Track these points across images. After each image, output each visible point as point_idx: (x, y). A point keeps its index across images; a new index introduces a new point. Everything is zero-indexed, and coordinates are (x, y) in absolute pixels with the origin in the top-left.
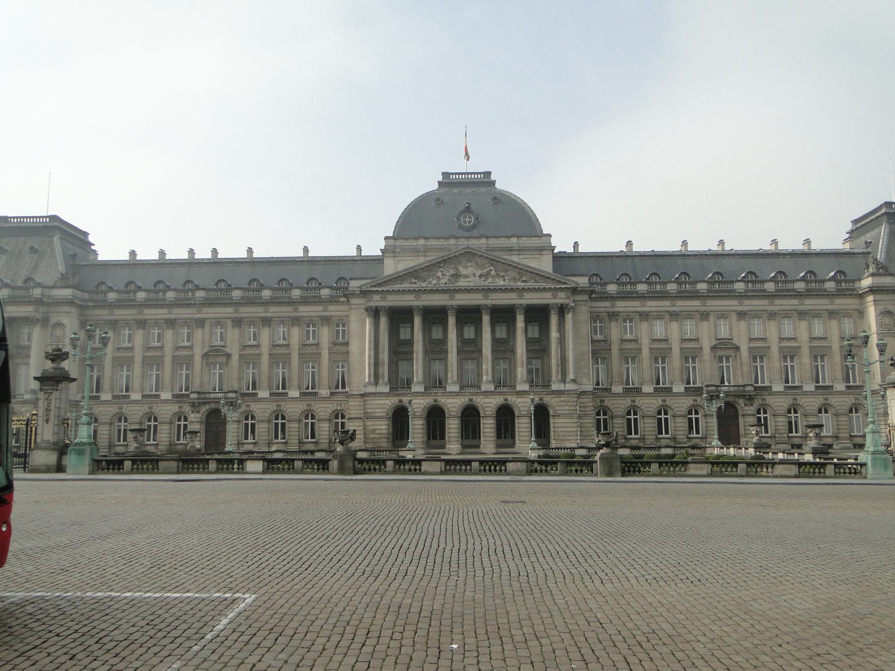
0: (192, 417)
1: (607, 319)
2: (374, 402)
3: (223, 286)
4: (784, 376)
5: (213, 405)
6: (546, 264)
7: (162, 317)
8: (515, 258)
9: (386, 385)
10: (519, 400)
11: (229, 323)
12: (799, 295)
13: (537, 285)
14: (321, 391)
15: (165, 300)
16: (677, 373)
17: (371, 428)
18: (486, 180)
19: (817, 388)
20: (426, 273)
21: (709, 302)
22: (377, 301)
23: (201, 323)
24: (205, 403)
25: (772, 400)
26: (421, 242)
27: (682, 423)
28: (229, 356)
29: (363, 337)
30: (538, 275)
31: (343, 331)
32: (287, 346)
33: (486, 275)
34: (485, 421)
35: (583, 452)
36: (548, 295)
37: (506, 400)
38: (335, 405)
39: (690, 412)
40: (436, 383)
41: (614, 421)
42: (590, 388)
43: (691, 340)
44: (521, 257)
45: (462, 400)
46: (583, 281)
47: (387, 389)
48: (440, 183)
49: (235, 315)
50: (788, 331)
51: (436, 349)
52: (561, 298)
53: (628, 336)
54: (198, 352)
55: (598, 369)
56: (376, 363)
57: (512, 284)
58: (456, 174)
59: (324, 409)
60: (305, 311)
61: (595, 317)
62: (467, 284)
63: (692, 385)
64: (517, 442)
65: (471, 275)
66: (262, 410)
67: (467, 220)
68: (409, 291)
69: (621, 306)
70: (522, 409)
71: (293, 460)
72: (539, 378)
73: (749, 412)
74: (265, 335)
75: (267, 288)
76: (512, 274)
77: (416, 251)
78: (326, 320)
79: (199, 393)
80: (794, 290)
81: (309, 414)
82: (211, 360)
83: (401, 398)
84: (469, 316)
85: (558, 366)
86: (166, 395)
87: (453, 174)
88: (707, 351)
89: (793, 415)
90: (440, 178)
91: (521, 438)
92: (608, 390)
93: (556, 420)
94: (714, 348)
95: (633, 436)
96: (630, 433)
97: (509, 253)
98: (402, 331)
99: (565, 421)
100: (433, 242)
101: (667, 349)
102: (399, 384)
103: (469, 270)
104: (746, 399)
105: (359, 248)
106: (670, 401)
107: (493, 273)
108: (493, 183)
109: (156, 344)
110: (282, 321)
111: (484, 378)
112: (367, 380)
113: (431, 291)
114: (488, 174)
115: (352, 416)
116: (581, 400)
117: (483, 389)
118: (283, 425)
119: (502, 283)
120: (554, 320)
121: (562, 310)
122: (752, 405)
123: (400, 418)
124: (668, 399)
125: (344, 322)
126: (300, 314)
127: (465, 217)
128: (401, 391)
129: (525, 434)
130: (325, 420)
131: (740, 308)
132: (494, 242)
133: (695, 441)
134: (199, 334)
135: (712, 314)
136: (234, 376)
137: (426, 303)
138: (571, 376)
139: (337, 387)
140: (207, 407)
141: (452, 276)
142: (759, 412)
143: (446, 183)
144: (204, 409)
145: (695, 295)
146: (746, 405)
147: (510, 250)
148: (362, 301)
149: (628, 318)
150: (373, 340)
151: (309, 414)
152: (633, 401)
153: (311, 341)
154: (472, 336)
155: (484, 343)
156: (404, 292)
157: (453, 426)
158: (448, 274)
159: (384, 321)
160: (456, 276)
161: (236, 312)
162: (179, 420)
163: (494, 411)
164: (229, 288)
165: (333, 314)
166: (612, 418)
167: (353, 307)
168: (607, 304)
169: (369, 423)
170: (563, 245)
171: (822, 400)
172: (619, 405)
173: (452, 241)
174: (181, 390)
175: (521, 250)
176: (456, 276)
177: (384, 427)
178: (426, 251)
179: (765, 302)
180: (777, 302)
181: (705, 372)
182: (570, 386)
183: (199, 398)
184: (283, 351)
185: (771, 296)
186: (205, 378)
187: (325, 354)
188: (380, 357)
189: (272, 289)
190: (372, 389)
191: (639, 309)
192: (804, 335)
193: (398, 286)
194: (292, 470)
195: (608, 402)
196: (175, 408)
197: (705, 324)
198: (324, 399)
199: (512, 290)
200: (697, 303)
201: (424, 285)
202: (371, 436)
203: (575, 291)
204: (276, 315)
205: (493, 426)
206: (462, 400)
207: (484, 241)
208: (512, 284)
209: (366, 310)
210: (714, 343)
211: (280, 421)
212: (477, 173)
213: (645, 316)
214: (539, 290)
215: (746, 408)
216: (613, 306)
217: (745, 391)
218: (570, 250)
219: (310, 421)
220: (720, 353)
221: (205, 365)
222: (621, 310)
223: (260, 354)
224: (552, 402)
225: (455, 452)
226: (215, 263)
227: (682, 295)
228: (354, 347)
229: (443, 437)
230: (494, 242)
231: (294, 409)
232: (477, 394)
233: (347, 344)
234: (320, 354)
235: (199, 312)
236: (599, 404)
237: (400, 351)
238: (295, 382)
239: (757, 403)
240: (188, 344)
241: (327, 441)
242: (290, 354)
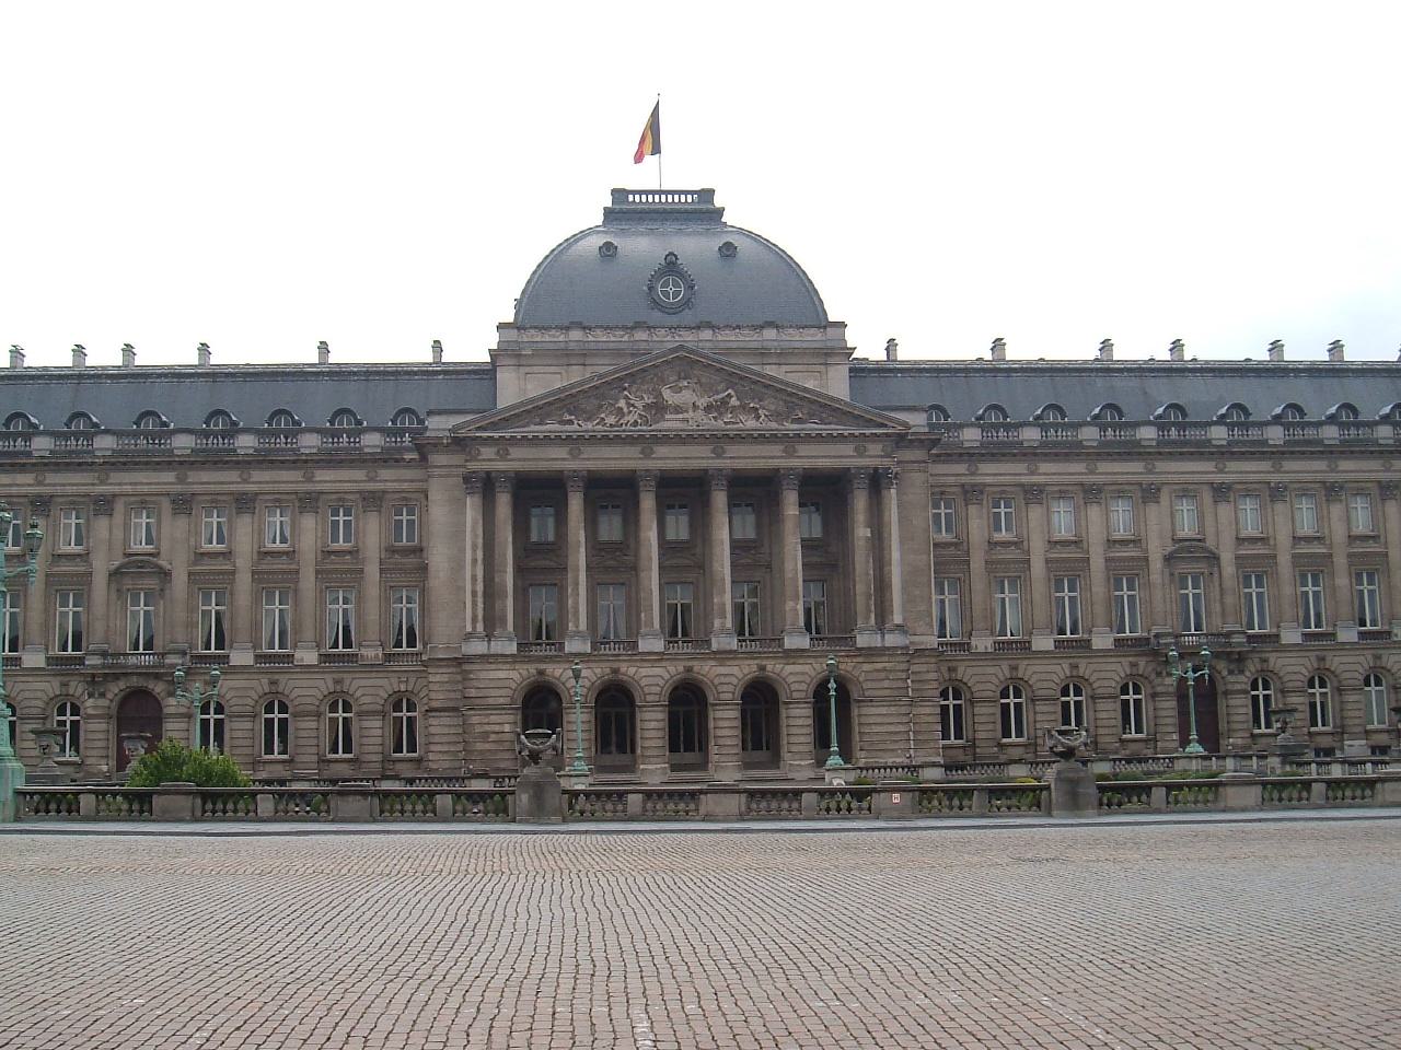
0: (89, 705)
1: (960, 501)
2: (483, 675)
3: (150, 425)
4: (1301, 614)
5: (135, 682)
6: (837, 385)
7: (24, 490)
8: (771, 371)
9: (511, 640)
10: (789, 668)
11: (166, 504)
12: (1329, 452)
13: (824, 429)
14: (364, 651)
15: (29, 454)
16: (1100, 609)
17: (478, 729)
18: (703, 207)
19: (1362, 635)
20: (596, 402)
21: (1161, 466)
22: (488, 460)
23: (104, 505)
24: (116, 677)
26: (576, 335)
27: (1109, 712)
28: (165, 575)
29: (457, 536)
30: (824, 407)
31: (411, 523)
32: (290, 554)
34: (719, 714)
35: (937, 773)
36: (848, 449)
37: (762, 668)
38: (394, 681)
39: (1125, 690)
40: (614, 639)
41: (977, 710)
42: (932, 641)
43: (1123, 542)
44: (784, 368)
45: (672, 669)
46: (917, 421)
47: (512, 648)
48: (608, 212)
49: (179, 488)
50: (1306, 524)
51: (614, 563)
52: (874, 456)
53: (1003, 535)
54: (101, 566)
55: (942, 602)
56: (491, 592)
57: (774, 425)
58: (640, 193)
59: (369, 690)
60: (326, 479)
61: (939, 495)
62: (679, 425)
63: (1128, 634)
64: (785, 755)
65: (688, 406)
66: (239, 691)
67: (671, 289)
68: (559, 440)
69: (991, 473)
70: (795, 687)
71: (432, 794)
72: (830, 625)
73: (1238, 687)
74: (244, 529)
75: (246, 431)
76: (771, 404)
77: (565, 356)
78: (372, 500)
79: (104, 654)
80: (1320, 442)
81: (339, 700)
82: (128, 583)
84: (684, 491)
85: (868, 597)
87: (634, 192)
88: (1156, 564)
89: (1317, 690)
90: (609, 204)
91: (794, 748)
92: (964, 646)
93: (865, 711)
94: (1169, 559)
95: (1013, 739)
96: (1006, 733)
97: (759, 360)
98: (534, 522)
99: (884, 710)
100: (601, 336)
101: (1324, 555)
102: (541, 636)
103: (686, 397)
104: (1231, 661)
105: (437, 346)
106: (1085, 669)
107: (734, 402)
108: (721, 211)
109: (73, 548)
110: (279, 502)
111: (717, 623)
112: (469, 629)
113: (606, 440)
114: (707, 194)
115: (434, 704)
116: (914, 668)
117: (715, 646)
118: (283, 723)
119: (751, 423)
120: (860, 502)
121: (877, 482)
122: (1242, 672)
123: (541, 706)
124: (1082, 664)
125: (415, 501)
126: (319, 487)
127: (666, 284)
128: (536, 652)
129: (802, 739)
130: (374, 713)
131: (1219, 478)
132: (728, 337)
133: (1134, 747)
134: (102, 524)
136: (181, 617)
137: (591, 465)
138: (898, 619)
139: (398, 644)
140: (122, 684)
141: (647, 407)
142: (1255, 687)
143: (621, 212)
144: (115, 689)
145: (1132, 451)
146: (1231, 672)
147: (762, 353)
148: (457, 459)
149: (1001, 495)
150: (480, 541)
151: (339, 700)
152: (1014, 668)
153: (341, 544)
154: (684, 535)
155: (717, 550)
156: (548, 440)
157: (652, 725)
158: (640, 404)
160: (659, 408)
161: (181, 480)
162: (62, 712)
163: (738, 693)
164: (165, 432)
165: (389, 486)
166: (972, 703)
167: (437, 471)
168: (961, 468)
169: (475, 720)
170: (867, 346)
171: (1370, 657)
172: (984, 679)
173: (641, 335)
174: (65, 649)
175: (784, 355)
176: (659, 408)
177: (507, 728)
178: (583, 355)
179: (1265, 465)
180: (1289, 465)
181: (1157, 606)
182: (892, 640)
183: (104, 666)
184: (280, 565)
185: (1277, 454)
186: (118, 623)
187: (372, 571)
188: (497, 580)
189: (259, 433)
190: (478, 647)
191: (1024, 480)
192: (1338, 533)
193: (533, 428)
194: (430, 813)
195: (965, 672)
196: (51, 687)
197: (1152, 509)
198: (371, 668)
199: (773, 439)
200: (1136, 467)
201: (589, 426)
202: (479, 746)
203: (902, 440)
204: (267, 488)
205: (738, 723)
206: (672, 669)
207: (707, 334)
208: (774, 425)
209: (466, 479)
210: (1170, 549)
211: (276, 716)
212: (686, 193)
214: (831, 439)
215: (1231, 678)
216: (972, 474)
217: (1230, 644)
218: (879, 355)
219: (340, 715)
220: (1182, 567)
221: (114, 596)
222: (989, 480)
223: (233, 573)
224: (856, 673)
225: (657, 780)
226: (132, 377)
227: (1106, 452)
228: (439, 558)
229: (703, 747)
230: (728, 337)
231: (306, 690)
232: (704, 658)
233: (419, 550)
234: (362, 571)
236: (947, 676)
237: (540, 565)
238: (309, 634)
239: (1252, 667)
240: (78, 549)
241: (379, 758)
242: (297, 572)
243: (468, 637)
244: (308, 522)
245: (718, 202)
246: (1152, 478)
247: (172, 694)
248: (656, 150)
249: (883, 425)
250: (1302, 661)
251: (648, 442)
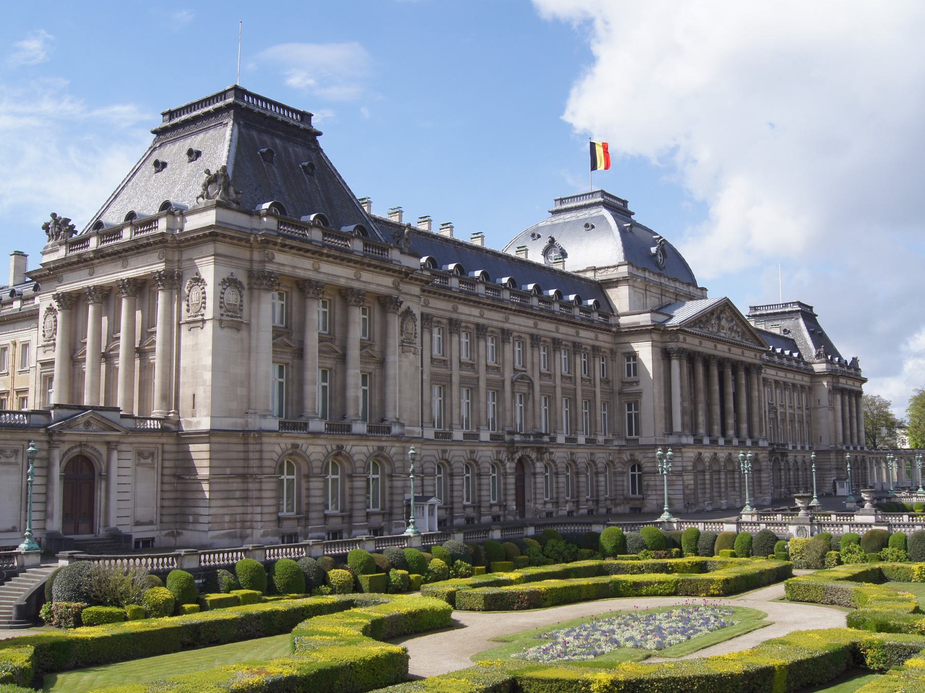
11: (528, 341)
33: (731, 329)
36: (752, 354)
49: (535, 331)
83: (700, 451)
86: (485, 436)
114: (625, 203)
119: (738, 338)
121: (759, 368)
159: (685, 363)
190: (684, 440)
201: (705, 330)
235: (507, 320)
243: (680, 435)
244: (579, 361)
245: (630, 208)
247: (537, 460)
249: (763, 346)
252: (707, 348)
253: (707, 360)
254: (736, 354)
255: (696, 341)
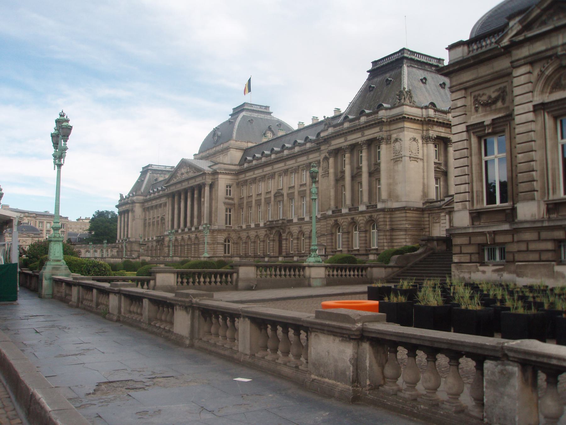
25: (293, 229)
33: (187, 173)
36: (200, 178)
88: (273, 199)
90: (231, 112)
94: (275, 196)
135: (276, 174)
168: (243, 176)
176: (182, 174)
197: (273, 180)
213: (254, 180)
216: (245, 177)
220: (278, 199)
222: (247, 178)
239: (287, 231)
246: (273, 171)
248: (250, 91)
250: (296, 228)
251: (180, 182)
252: (179, 187)
253: (179, 193)
254: (193, 183)
255: (174, 187)
